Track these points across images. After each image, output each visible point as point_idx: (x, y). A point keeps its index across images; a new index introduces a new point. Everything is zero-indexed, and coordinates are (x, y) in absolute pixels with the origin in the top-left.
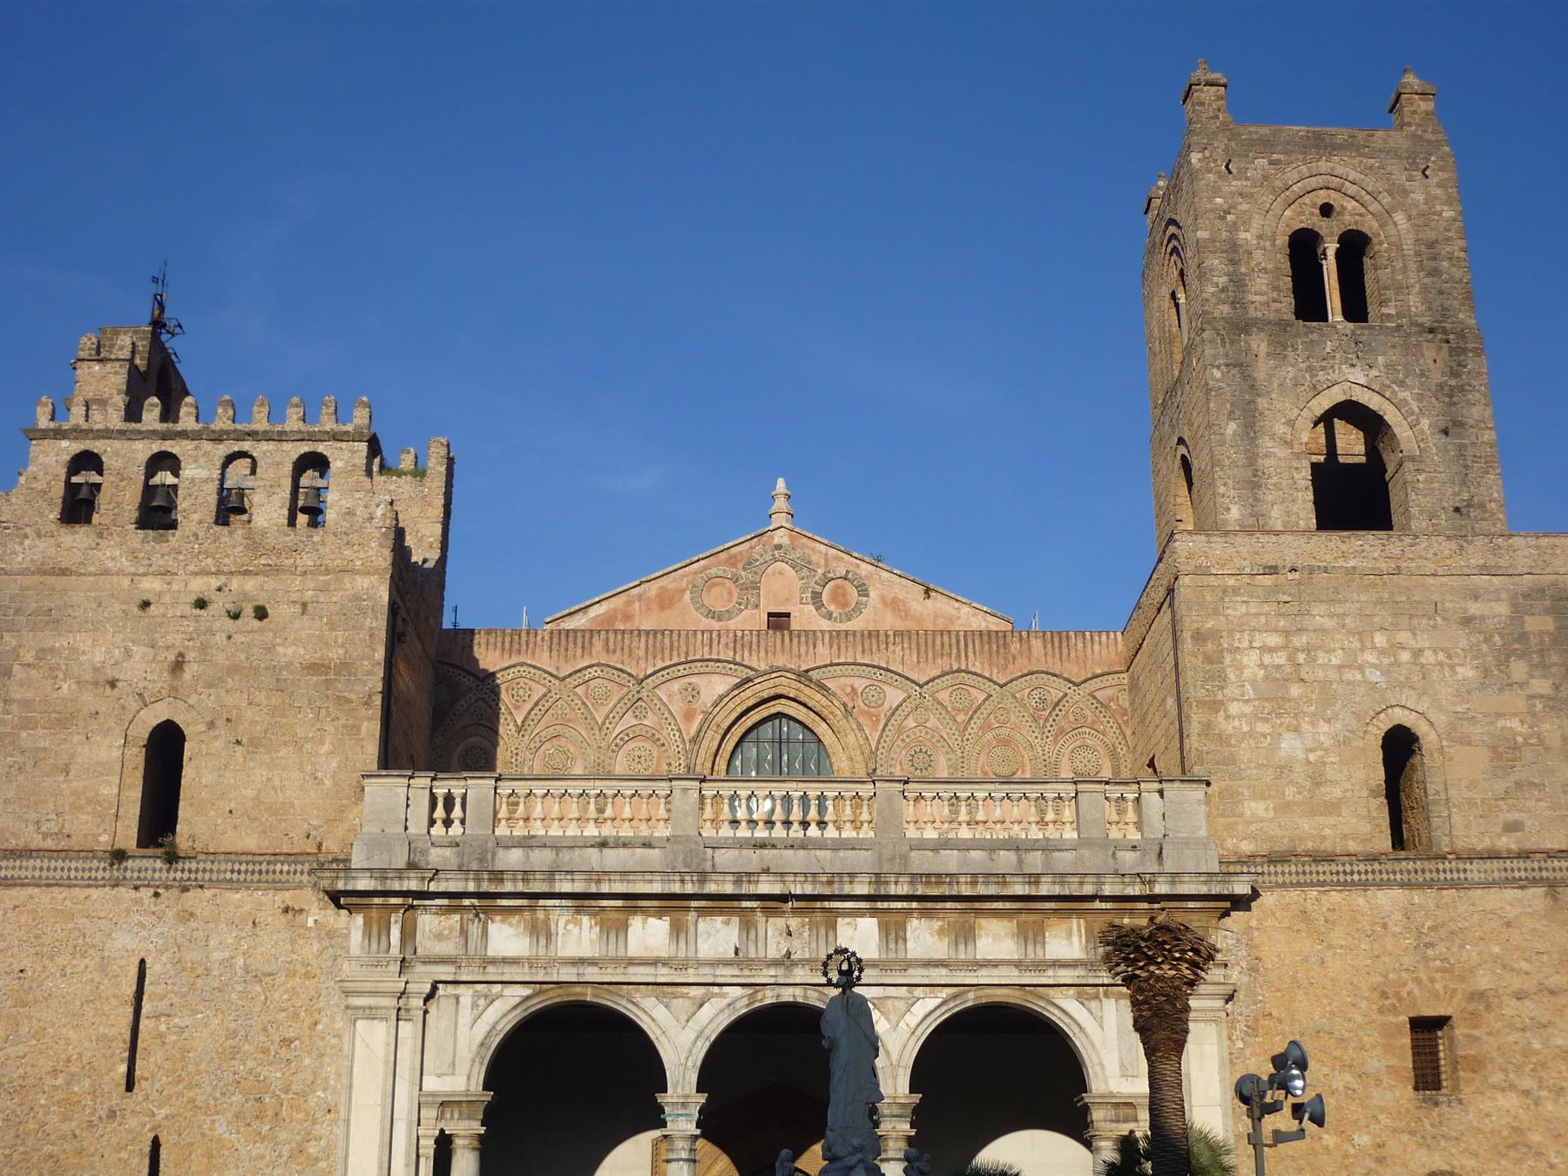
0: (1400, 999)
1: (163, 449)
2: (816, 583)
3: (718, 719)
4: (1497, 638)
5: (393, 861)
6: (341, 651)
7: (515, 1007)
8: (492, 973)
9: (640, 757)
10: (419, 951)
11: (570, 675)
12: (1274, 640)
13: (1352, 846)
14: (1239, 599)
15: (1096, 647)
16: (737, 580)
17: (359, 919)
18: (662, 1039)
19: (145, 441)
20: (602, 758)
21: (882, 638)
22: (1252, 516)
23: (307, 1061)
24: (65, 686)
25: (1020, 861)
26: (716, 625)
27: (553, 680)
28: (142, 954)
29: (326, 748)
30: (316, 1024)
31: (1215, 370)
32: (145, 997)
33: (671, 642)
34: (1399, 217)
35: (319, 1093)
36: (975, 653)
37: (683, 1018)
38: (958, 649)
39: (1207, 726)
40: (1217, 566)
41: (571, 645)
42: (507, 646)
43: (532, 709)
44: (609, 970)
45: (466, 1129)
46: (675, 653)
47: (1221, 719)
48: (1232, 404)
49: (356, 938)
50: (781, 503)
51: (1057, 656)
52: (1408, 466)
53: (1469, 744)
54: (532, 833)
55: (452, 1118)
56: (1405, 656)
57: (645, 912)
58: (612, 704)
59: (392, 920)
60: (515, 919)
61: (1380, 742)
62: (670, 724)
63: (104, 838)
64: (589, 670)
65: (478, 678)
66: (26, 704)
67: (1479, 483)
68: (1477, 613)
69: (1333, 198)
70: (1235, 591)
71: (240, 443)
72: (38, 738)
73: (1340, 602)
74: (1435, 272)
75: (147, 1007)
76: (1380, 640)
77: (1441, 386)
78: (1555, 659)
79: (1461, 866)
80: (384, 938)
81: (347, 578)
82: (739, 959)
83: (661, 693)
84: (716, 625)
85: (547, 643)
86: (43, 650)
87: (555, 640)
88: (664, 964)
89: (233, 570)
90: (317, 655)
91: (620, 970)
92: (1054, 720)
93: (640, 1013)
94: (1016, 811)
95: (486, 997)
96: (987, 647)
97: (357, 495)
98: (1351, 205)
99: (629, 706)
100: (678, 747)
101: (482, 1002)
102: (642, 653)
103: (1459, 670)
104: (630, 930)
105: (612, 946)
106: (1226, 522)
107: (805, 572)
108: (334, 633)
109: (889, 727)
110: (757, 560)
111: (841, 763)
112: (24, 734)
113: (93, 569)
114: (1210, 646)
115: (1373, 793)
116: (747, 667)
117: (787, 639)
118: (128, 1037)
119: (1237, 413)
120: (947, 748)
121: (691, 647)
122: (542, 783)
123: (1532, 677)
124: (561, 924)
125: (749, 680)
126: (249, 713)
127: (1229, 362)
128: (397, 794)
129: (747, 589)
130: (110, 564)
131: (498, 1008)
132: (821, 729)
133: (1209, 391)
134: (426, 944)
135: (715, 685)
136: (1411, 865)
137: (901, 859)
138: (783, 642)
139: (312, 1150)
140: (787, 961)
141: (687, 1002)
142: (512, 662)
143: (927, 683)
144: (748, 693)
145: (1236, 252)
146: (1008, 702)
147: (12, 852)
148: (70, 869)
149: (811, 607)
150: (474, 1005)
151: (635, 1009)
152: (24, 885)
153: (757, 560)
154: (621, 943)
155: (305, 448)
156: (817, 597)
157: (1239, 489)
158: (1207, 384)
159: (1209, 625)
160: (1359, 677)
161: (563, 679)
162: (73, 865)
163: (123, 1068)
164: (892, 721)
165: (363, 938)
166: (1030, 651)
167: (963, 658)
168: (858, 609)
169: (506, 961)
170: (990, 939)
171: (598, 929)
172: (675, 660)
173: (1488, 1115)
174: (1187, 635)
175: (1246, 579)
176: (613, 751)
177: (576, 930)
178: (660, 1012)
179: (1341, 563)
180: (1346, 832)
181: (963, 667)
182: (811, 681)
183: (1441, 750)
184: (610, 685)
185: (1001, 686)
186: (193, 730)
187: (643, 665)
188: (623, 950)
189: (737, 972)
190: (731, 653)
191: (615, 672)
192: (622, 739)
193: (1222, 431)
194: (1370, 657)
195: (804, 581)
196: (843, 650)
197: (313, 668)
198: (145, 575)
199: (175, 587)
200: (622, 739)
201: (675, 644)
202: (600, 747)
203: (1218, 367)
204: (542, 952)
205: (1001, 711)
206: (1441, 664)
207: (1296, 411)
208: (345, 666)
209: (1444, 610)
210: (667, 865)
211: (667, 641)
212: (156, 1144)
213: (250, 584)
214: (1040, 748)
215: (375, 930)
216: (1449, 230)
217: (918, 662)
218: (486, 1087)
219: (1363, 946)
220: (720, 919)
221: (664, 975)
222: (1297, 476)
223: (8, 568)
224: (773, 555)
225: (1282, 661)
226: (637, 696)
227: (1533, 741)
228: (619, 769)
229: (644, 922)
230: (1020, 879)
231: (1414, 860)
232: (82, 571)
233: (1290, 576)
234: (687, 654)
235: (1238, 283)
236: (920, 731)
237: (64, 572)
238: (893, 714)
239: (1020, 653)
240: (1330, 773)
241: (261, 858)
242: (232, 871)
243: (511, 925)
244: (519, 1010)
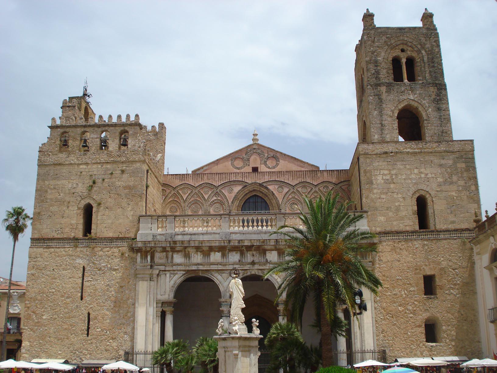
0: (421, 270)
1: (85, 130)
3: (238, 197)
4: (449, 170)
7: (181, 277)
8: (175, 268)
12: (386, 172)
13: (408, 229)
15: (342, 174)
17: (139, 254)
18: (220, 284)
19: (80, 128)
21: (283, 173)
23: (127, 292)
24: (61, 195)
28: (83, 265)
29: (129, 209)
30: (129, 282)
31: (371, 97)
32: (85, 276)
33: (225, 176)
34: (423, 52)
35: (130, 300)
36: (308, 177)
37: (225, 279)
38: (304, 176)
39: (367, 198)
41: (198, 178)
42: (181, 179)
43: (188, 196)
44: (206, 266)
45: (169, 309)
46: (226, 179)
48: (376, 106)
49: (139, 259)
51: (331, 177)
52: (425, 122)
53: (441, 199)
55: (165, 306)
56: (423, 176)
57: (215, 251)
59: (148, 254)
60: (180, 254)
61: (416, 200)
63: (73, 235)
65: (173, 187)
66: (51, 199)
67: (445, 126)
68: (444, 163)
69: (405, 47)
71: (105, 128)
72: (54, 209)
73: (405, 161)
74: (433, 67)
75: (85, 278)
76: (416, 171)
77: (435, 99)
78: (465, 174)
79: (438, 233)
80: (146, 259)
82: (240, 262)
84: (238, 171)
85: (192, 177)
86: (55, 185)
87: (194, 177)
88: (220, 265)
89: (104, 162)
90: (127, 184)
91: (208, 266)
93: (215, 278)
95: (173, 274)
96: (311, 175)
98: (409, 49)
101: (172, 275)
102: (217, 179)
103: (439, 179)
104: (211, 256)
105: (206, 260)
106: (374, 139)
112: (51, 208)
113: (67, 163)
114: (368, 174)
115: (414, 214)
116: (246, 182)
117: (257, 174)
118: (80, 285)
121: (231, 177)
123: (459, 180)
124: (192, 255)
125: (246, 186)
126: (110, 200)
130: (72, 162)
131: (177, 276)
132: (266, 199)
133: (369, 103)
134: (157, 260)
135: (237, 189)
136: (424, 233)
138: (255, 175)
139: (129, 315)
140: (253, 263)
141: (226, 274)
142: (182, 183)
144: (246, 190)
145: (377, 63)
147: (49, 239)
148: (64, 243)
150: (170, 277)
151: (212, 277)
152: (52, 247)
154: (209, 259)
155: (122, 128)
158: (369, 101)
159: (368, 169)
160: (410, 182)
161: (196, 187)
162: (65, 242)
163: (80, 294)
166: (323, 176)
167: (305, 178)
168: (277, 165)
169: (178, 265)
173: (444, 301)
174: (362, 171)
175: (379, 156)
177: (197, 256)
178: (219, 277)
179: (405, 150)
180: (406, 225)
181: (305, 181)
182: (263, 185)
183: (433, 201)
186: (94, 205)
187: (218, 182)
189: (239, 266)
190: (241, 179)
194: (413, 176)
196: (272, 178)
197: (125, 188)
198: (81, 164)
199: (89, 167)
201: (226, 177)
203: (372, 96)
204: (188, 262)
206: (433, 177)
207: (394, 108)
208: (134, 187)
209: (434, 162)
211: (224, 176)
212: (89, 314)
213: (109, 166)
216: (437, 55)
217: (293, 179)
218: (175, 297)
219: (411, 256)
220: (235, 252)
221: (220, 267)
222: (394, 126)
223: (45, 163)
225: (388, 178)
226: (216, 191)
227: (459, 198)
228: (212, 212)
229: (215, 253)
231: (425, 232)
232: (65, 163)
233: (391, 154)
234: (229, 180)
235: (378, 72)
237: (60, 164)
240: (401, 208)
241: (113, 239)
242: (106, 242)
244: (183, 277)
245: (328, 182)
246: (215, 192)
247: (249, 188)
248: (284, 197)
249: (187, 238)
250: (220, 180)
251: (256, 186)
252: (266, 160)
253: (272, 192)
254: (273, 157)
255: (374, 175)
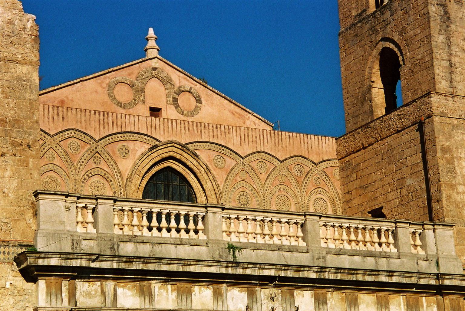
2: (175, 92)
3: (140, 168)
5: (62, 247)
6: (13, 112)
9: (98, 187)
10: (78, 304)
11: (57, 134)
14: (459, 131)
16: (133, 86)
17: (42, 283)
20: (77, 186)
22: (451, 87)
25: (377, 263)
26: (124, 111)
27: (46, 135)
29: (8, 173)
36: (268, 142)
40: (450, 113)
46: (115, 126)
47: (455, 194)
50: (152, 43)
54: (135, 234)
58: (81, 154)
59: (63, 285)
62: (114, 169)
64: (67, 132)
70: (458, 127)
80: (59, 296)
81: (12, 65)
83: (108, 149)
92: (306, 183)
94: (284, 229)
97: (14, 12)
99: (91, 156)
100: (119, 182)
104: (193, 293)
105: (184, 303)
107: (169, 86)
108: (7, 100)
109: (228, 180)
110: (143, 75)
111: (201, 198)
114: (448, 155)
119: (443, 31)
120: (256, 194)
122: (138, 204)
125: (156, 146)
127: (439, 3)
128: (59, 206)
129: (138, 91)
132: (191, 178)
137: (323, 259)
143: (246, 157)
146: (285, 172)
149: (173, 107)
153: (143, 75)
154: (189, 301)
156: (175, 100)
157: (445, 72)
159: (447, 144)
164: (230, 177)
165: (47, 295)
168: (197, 110)
170: (365, 306)
171: (175, 293)
172: (115, 131)
176: (83, 182)
181: (262, 150)
182: (189, 150)
184: (79, 142)
185: (281, 162)
188: (190, 305)
191: (82, 134)
192: (88, 175)
193: (436, 40)
195: (168, 91)
200: (88, 175)
202: (75, 180)
203: (434, 5)
205: (281, 176)
208: (16, 122)
210: (210, 256)
211: (110, 118)
214: (300, 198)
215: (53, 290)
220: (238, 289)
224: (152, 73)
230: (385, 273)
236: (243, 183)
238: (230, 173)
239: (290, 143)
243: (129, 289)
245: (302, 157)
246: (94, 152)
247: (161, 152)
248: (227, 179)
249: (144, 250)
250: (102, 128)
251: (174, 149)
252: (176, 96)
253: (206, 166)
254: (189, 92)
255: (457, 158)
